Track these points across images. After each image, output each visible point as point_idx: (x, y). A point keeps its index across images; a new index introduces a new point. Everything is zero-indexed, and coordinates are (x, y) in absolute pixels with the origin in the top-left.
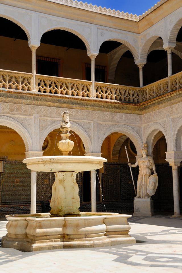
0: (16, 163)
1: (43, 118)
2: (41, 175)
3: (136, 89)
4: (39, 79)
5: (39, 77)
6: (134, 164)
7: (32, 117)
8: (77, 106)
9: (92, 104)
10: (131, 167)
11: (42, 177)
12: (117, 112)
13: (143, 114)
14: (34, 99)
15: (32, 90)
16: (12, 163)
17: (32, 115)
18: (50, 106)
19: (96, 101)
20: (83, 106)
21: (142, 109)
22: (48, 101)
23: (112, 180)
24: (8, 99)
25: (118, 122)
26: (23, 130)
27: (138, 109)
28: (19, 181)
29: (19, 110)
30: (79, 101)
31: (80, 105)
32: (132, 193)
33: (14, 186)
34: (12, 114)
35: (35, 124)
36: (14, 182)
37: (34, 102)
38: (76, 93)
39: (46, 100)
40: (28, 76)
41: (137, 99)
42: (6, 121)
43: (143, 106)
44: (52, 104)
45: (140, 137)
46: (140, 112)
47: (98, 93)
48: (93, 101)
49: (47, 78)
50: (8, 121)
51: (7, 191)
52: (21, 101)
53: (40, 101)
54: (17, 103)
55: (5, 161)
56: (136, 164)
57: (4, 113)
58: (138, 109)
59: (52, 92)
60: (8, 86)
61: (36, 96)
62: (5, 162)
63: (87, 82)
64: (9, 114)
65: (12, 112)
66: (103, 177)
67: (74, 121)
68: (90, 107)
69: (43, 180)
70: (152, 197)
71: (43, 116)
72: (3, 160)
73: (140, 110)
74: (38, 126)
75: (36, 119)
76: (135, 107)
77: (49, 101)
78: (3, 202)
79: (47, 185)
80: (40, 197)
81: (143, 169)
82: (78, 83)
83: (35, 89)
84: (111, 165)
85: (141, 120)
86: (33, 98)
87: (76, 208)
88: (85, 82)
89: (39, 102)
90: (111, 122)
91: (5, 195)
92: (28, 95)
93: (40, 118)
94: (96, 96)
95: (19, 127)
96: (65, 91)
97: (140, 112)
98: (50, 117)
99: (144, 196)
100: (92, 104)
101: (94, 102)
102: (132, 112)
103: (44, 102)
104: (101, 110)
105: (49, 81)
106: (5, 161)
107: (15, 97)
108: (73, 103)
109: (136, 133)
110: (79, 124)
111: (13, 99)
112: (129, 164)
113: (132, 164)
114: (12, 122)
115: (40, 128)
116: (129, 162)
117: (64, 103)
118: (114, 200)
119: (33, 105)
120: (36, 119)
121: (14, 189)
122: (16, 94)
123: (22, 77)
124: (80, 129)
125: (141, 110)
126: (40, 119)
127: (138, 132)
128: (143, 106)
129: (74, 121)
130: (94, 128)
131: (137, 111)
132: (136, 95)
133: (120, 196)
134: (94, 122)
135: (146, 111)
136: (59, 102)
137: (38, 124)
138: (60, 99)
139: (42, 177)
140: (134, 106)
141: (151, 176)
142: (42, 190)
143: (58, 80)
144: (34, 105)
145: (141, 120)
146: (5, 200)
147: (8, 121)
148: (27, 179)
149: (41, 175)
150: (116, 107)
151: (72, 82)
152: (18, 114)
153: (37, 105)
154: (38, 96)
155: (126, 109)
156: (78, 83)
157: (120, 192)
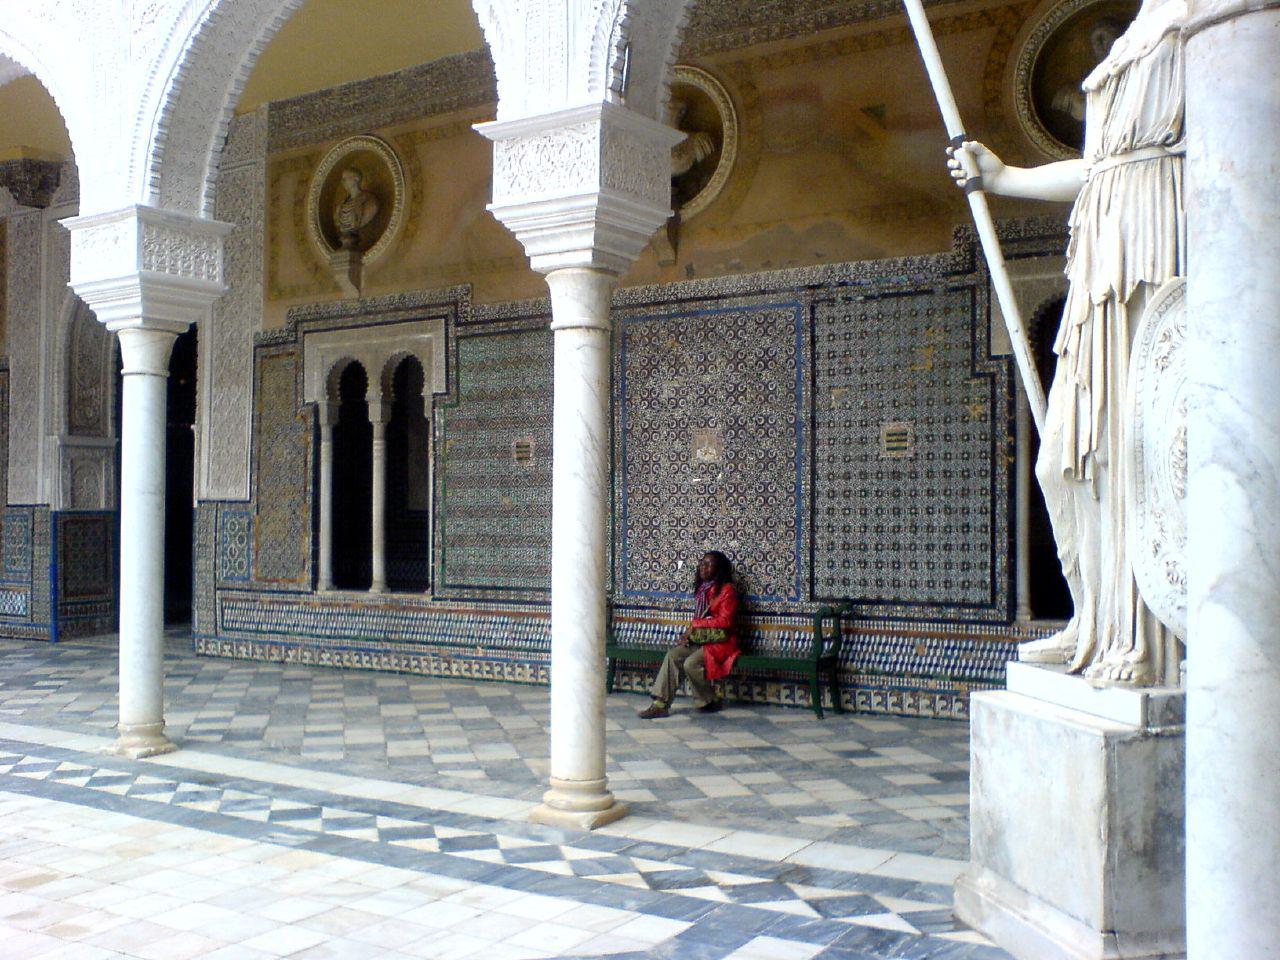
0: (516, 326)
2: (663, 397)
11: (678, 414)
16: (491, 328)
28: (532, 444)
33: (504, 483)
36: (506, 452)
51: (469, 513)
55: (456, 316)
62: (458, 324)
69: (681, 431)
72: (445, 317)
78: (452, 587)
79: (709, 469)
80: (665, 562)
91: (460, 540)
106: (456, 316)
112: (961, 162)
121: (506, 501)
142: (679, 513)
146: (462, 570)
149: (663, 397)
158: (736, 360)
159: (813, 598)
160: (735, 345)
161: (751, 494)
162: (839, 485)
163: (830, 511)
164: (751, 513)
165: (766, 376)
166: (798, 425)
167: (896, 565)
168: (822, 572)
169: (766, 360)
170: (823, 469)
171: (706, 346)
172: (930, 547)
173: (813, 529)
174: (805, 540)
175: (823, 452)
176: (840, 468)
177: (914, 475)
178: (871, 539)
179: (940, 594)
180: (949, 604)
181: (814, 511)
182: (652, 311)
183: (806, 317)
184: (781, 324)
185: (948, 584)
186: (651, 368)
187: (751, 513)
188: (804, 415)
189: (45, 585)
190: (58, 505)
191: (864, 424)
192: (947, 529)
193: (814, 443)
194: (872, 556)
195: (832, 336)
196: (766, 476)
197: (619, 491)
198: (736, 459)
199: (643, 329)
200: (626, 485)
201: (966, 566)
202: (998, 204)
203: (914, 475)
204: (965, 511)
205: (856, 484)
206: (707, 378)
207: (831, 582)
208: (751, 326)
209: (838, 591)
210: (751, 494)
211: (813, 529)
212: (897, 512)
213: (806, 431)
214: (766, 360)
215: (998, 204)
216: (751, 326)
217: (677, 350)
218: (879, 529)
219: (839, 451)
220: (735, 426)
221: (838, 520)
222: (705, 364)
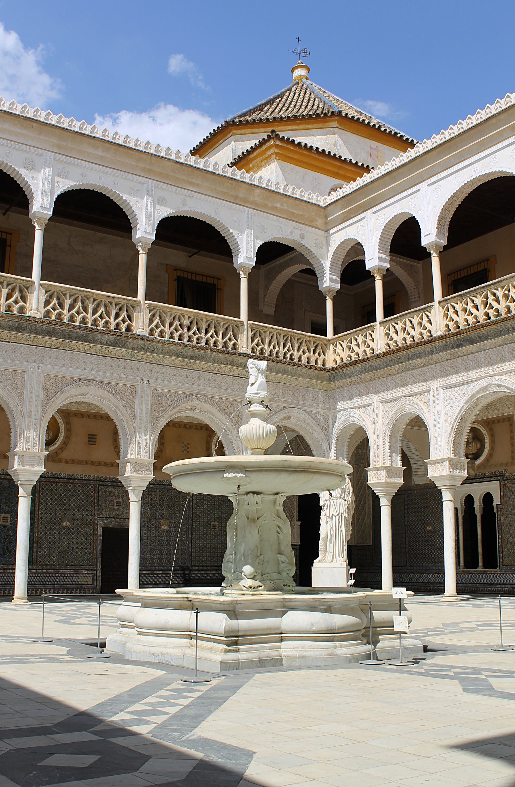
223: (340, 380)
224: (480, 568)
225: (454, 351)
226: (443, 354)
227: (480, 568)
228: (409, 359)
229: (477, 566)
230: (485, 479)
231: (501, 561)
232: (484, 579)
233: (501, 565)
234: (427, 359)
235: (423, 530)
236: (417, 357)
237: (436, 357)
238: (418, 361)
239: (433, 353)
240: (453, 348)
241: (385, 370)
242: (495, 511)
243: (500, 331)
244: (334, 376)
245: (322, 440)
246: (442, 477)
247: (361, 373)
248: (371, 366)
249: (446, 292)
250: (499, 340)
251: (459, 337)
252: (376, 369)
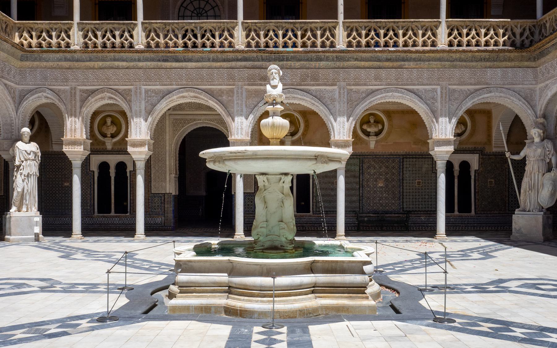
1: (353, 87)
3: (528, 23)
4: (348, 27)
5: (348, 25)
6: (518, 153)
7: (335, 87)
8: (411, 63)
9: (447, 58)
10: (511, 159)
11: (375, 177)
12: (486, 68)
13: (539, 66)
14: (339, 59)
15: (337, 46)
17: (335, 85)
18: (364, 68)
19: (449, 51)
20: (422, 63)
21: (536, 57)
22: (361, 61)
23: (493, 180)
24: (298, 64)
25: (487, 84)
26: (321, 107)
27: (530, 59)
29: (315, 79)
30: (414, 56)
31: (416, 61)
32: (512, 204)
34: (305, 85)
35: (340, 97)
37: (338, 63)
38: (410, 42)
39: (356, 59)
40: (330, 25)
41: (529, 40)
42: (295, 96)
43: (537, 52)
44: (367, 64)
45: (533, 107)
46: (534, 63)
47: (451, 38)
48: (443, 51)
49: (361, 24)
50: (299, 96)
52: (317, 65)
53: (348, 61)
54: (312, 68)
56: (522, 154)
57: (292, 85)
58: (530, 59)
59: (371, 45)
60: (299, 43)
61: (340, 54)
63: (431, 22)
64: (301, 85)
65: (305, 83)
66: (477, 175)
67: (405, 89)
68: (434, 63)
69: (376, 181)
70: (548, 209)
71: (354, 85)
73: (532, 59)
74: (345, 100)
75: (342, 90)
76: (522, 56)
77: (362, 60)
79: (382, 187)
81: (532, 162)
82: (416, 26)
83: (341, 43)
84: (491, 157)
85: (536, 77)
86: (336, 57)
87: (286, 238)
88: (428, 22)
89: (346, 64)
90: (475, 84)
92: (327, 54)
93: (349, 87)
94: (447, 42)
95: (316, 103)
96: (392, 41)
97: (533, 64)
98: (365, 85)
99: (532, 207)
100: (441, 57)
101: (441, 54)
102: (517, 63)
103: (355, 63)
104: (455, 67)
105: (365, 27)
107: (308, 60)
108: (404, 60)
109: (524, 101)
110: (414, 93)
111: (305, 63)
113: (512, 154)
114: (305, 98)
115: (348, 103)
116: (507, 150)
117: (388, 60)
118: (496, 212)
119: (337, 68)
120: (342, 90)
122: (308, 54)
123: (321, 28)
124: (416, 100)
125: (535, 59)
126: (348, 90)
127: (529, 99)
128: (537, 52)
129: (405, 89)
130: (442, 97)
131: (527, 61)
132: (527, 33)
133: (507, 205)
134: (442, 88)
135: (543, 60)
136: (379, 60)
137: (346, 97)
138: (380, 55)
139: (375, 177)
140: (521, 54)
141: (548, 175)
142: (375, 195)
143: (379, 25)
144: (339, 68)
145: (536, 77)
147: (299, 96)
148: (352, 179)
150: (485, 59)
151: (404, 24)
152: (313, 85)
153: (343, 68)
154: (342, 54)
155: (505, 60)
156: (416, 26)
157: (507, 199)
158: (387, 167)
159: (403, 211)
160: (387, 164)
161: (390, 192)
162: (408, 191)
163: (406, 195)
164: (390, 196)
165: (393, 171)
166: (400, 180)
167: (419, 205)
168: (405, 206)
169: (393, 167)
170: (405, 188)
171: (381, 164)
172: (425, 201)
173: (403, 198)
174: (401, 200)
175: (405, 185)
176: (408, 188)
177: (422, 189)
178: (414, 200)
179: (427, 209)
180: (428, 211)
181: (403, 195)
182: (369, 157)
183: (402, 160)
184: (396, 161)
185: (428, 207)
186: (369, 167)
187: (390, 196)
188: (401, 178)
189: (170, 215)
190: (174, 194)
191: (413, 180)
192: (428, 198)
193: (403, 183)
194: (414, 203)
195: (406, 164)
196: (393, 189)
197: (361, 191)
198: (387, 186)
199: (367, 160)
200: (362, 190)
201: (431, 205)
202: (511, 160)
203: (422, 189)
204: (431, 195)
205: (411, 191)
206: (381, 171)
207: (406, 208)
208: (390, 161)
209: (408, 209)
210: (390, 192)
211: (403, 198)
212: (419, 195)
213: (401, 181)
214: (393, 167)
215: (511, 159)
216: (390, 161)
217: (375, 165)
218: (416, 199)
219: (408, 185)
220: (387, 180)
221: (408, 197)
222: (380, 168)
223: (32, 61)
224: (113, 213)
225: (159, 63)
226: (149, 63)
227: (113, 213)
228: (115, 60)
229: (110, 212)
230: (121, 153)
231: (132, 209)
232: (116, 221)
233: (132, 212)
234: (132, 64)
235: (60, 186)
236: (123, 61)
237: (141, 64)
238: (124, 64)
239: (139, 60)
240: (159, 61)
241: (88, 63)
242: (128, 175)
243: (202, 58)
244: (27, 57)
245: (13, 109)
246: (140, 153)
247: (60, 60)
248: (73, 57)
249: (146, 16)
250: (199, 64)
251: (169, 54)
252: (77, 61)
